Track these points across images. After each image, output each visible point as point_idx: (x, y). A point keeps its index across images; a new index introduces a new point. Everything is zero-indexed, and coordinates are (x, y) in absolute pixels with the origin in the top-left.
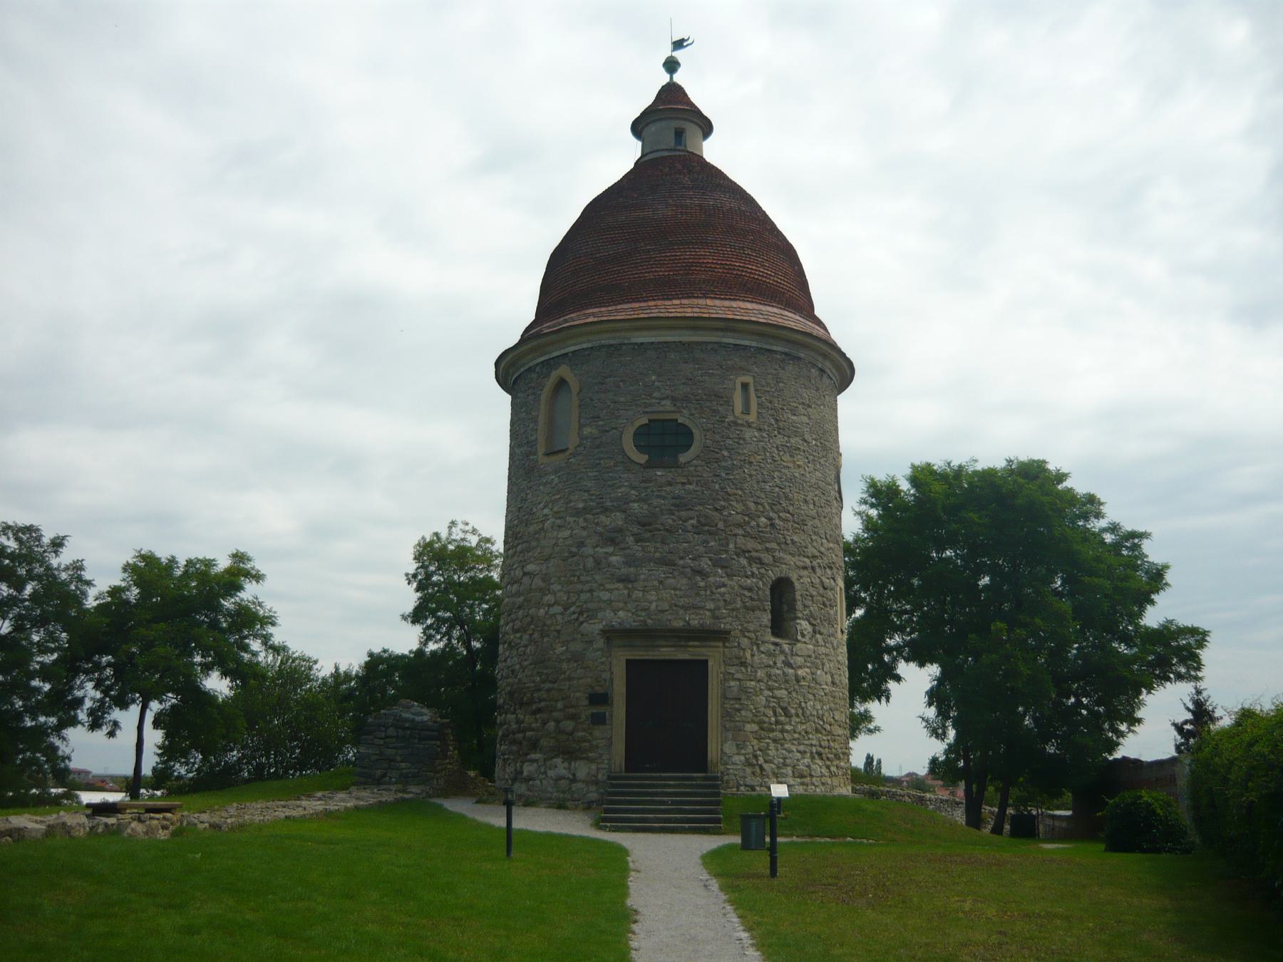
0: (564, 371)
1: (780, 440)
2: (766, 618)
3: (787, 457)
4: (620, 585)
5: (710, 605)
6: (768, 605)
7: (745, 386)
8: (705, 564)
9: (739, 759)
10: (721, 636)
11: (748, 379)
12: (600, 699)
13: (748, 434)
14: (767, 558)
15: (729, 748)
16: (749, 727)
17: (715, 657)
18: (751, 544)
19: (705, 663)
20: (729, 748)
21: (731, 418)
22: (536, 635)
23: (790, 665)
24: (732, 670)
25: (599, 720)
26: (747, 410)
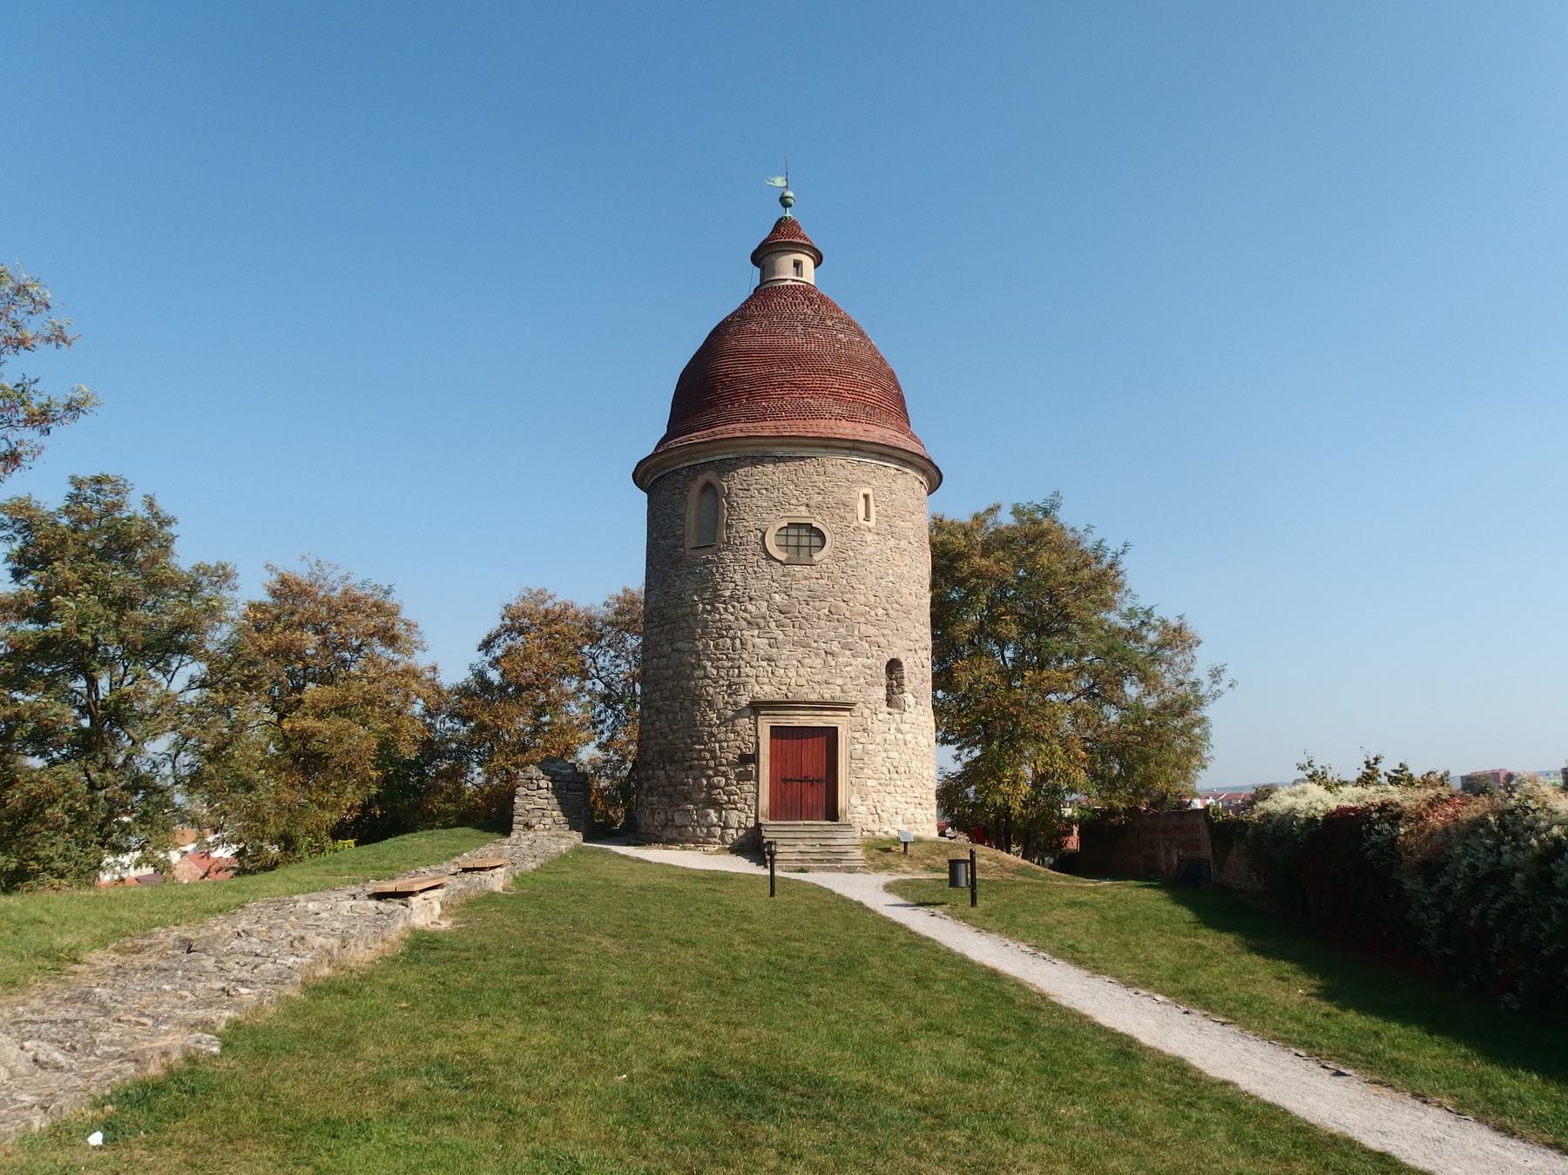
0: (710, 476)
1: (892, 542)
2: (882, 693)
3: (897, 557)
4: (765, 664)
5: (840, 681)
6: (884, 681)
7: (866, 497)
8: (835, 647)
9: (863, 809)
10: (847, 707)
11: (868, 491)
12: (749, 759)
13: (869, 537)
14: (882, 641)
15: (855, 800)
16: (870, 783)
17: (840, 721)
18: (871, 630)
19: (831, 734)
20: (855, 800)
21: (855, 524)
22: (687, 704)
23: (899, 731)
24: (857, 735)
25: (743, 777)
26: (867, 518)
